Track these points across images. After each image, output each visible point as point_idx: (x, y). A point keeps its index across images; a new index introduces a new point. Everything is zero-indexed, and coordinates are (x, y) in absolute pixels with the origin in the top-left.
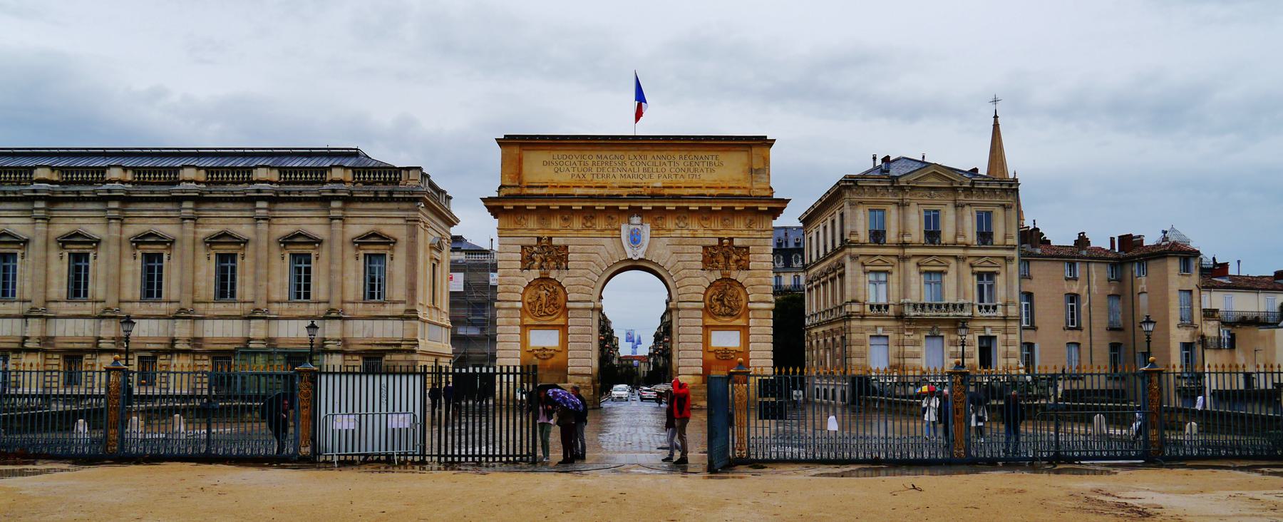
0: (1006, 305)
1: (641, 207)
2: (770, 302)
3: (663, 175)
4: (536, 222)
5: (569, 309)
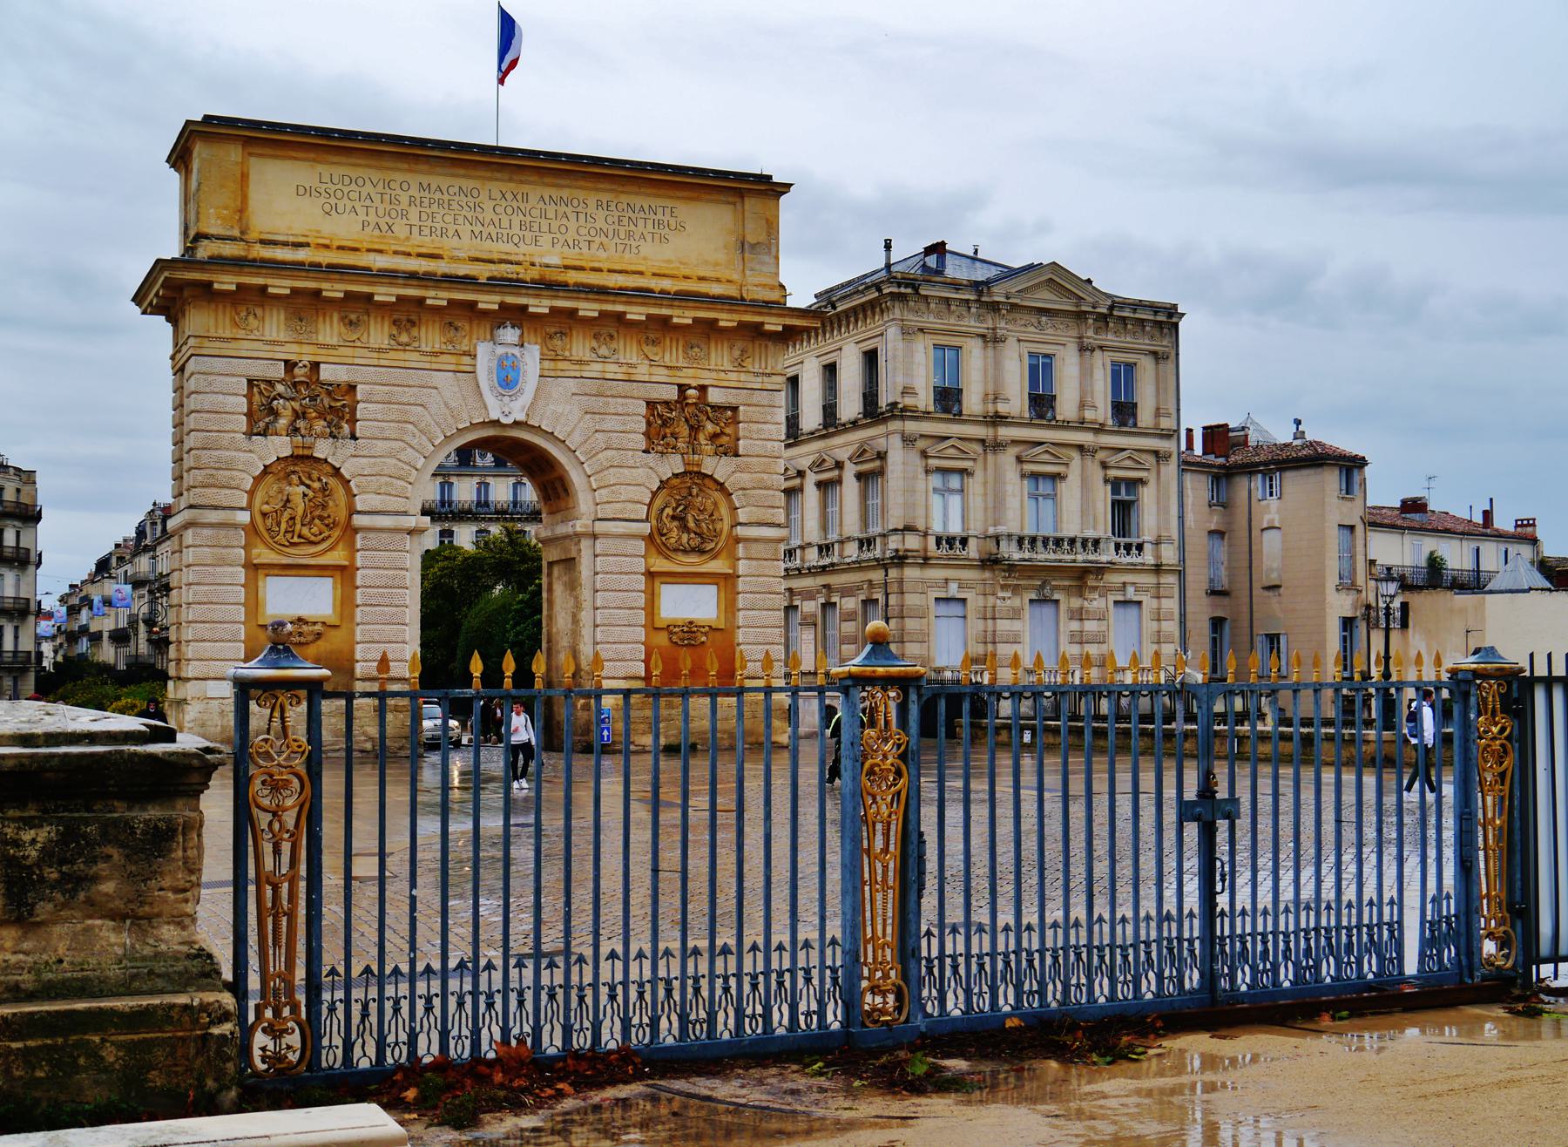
0: (1157, 543)
1: (526, 307)
2: (779, 526)
3: (562, 241)
4: (282, 326)
5: (356, 531)
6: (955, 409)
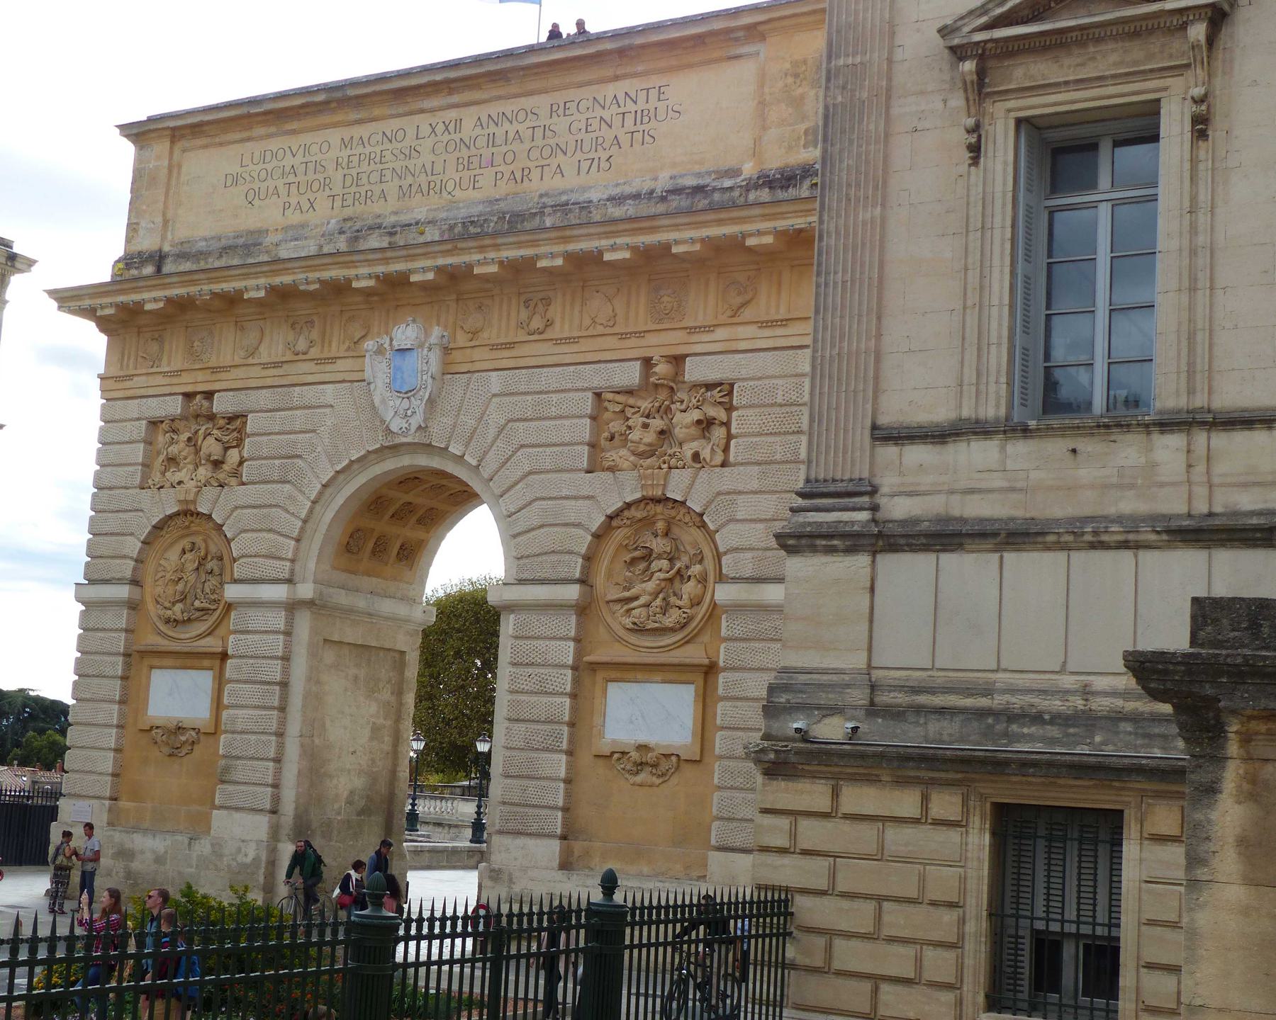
3: (507, 176)
5: (229, 607)
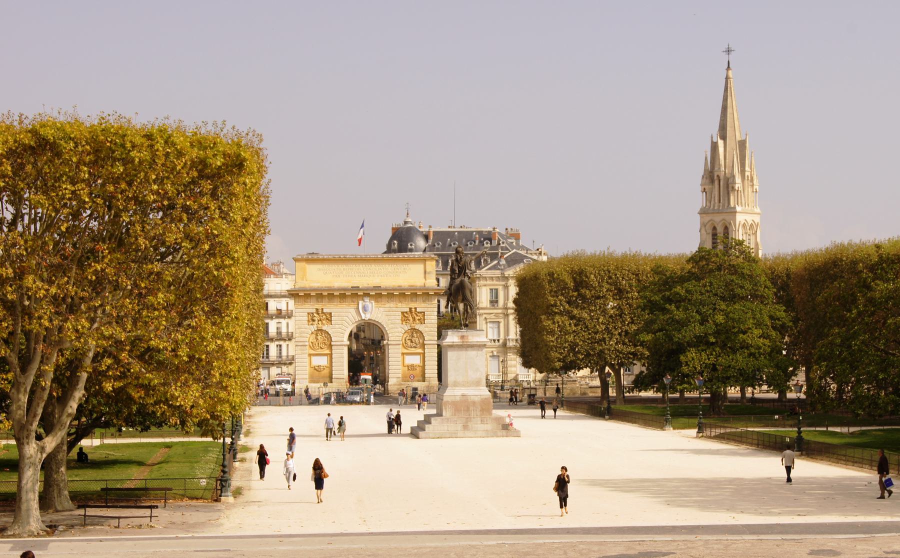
6: (496, 305)
